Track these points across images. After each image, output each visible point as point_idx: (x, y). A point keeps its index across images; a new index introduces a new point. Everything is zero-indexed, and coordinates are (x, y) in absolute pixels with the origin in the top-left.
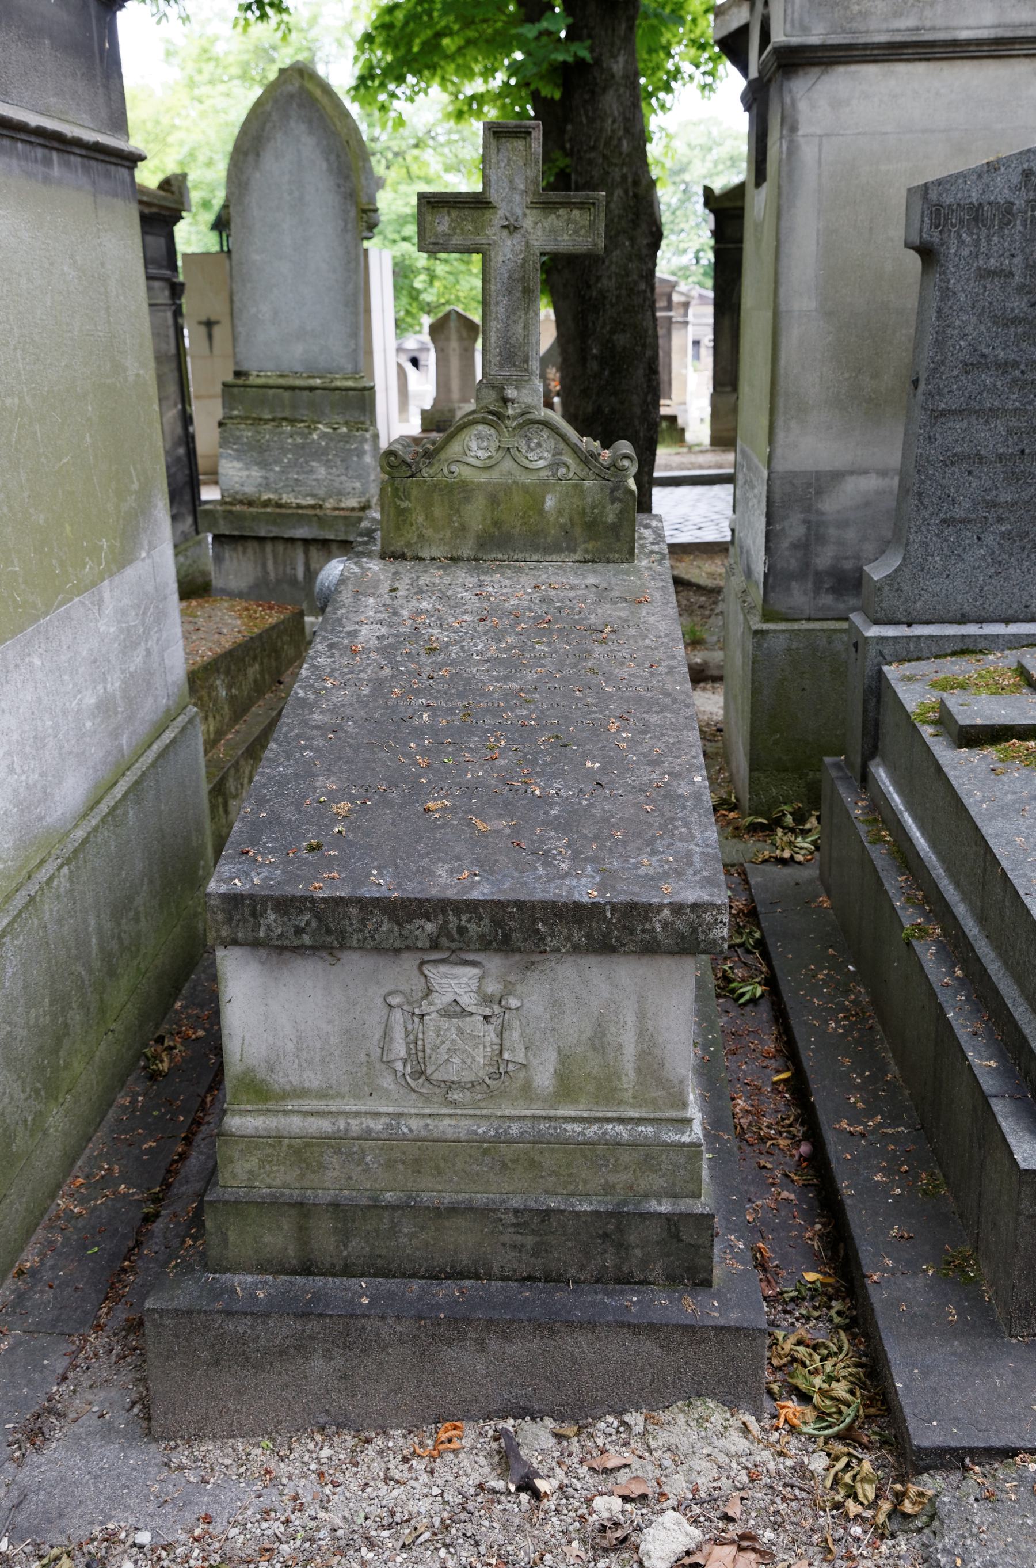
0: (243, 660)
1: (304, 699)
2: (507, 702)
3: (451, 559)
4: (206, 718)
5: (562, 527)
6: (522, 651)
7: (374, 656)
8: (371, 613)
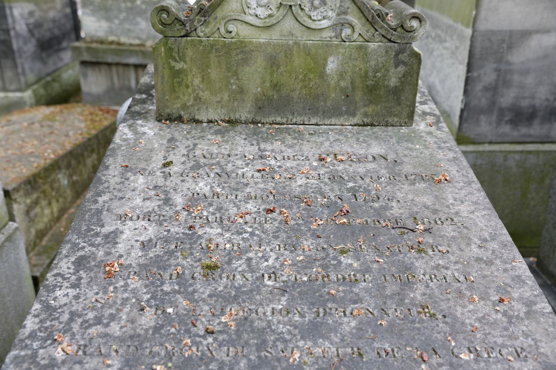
0: (82, 155)
3: (228, 122)
4: (50, 204)
5: (343, 90)
6: (325, 267)
7: (135, 283)
8: (138, 201)
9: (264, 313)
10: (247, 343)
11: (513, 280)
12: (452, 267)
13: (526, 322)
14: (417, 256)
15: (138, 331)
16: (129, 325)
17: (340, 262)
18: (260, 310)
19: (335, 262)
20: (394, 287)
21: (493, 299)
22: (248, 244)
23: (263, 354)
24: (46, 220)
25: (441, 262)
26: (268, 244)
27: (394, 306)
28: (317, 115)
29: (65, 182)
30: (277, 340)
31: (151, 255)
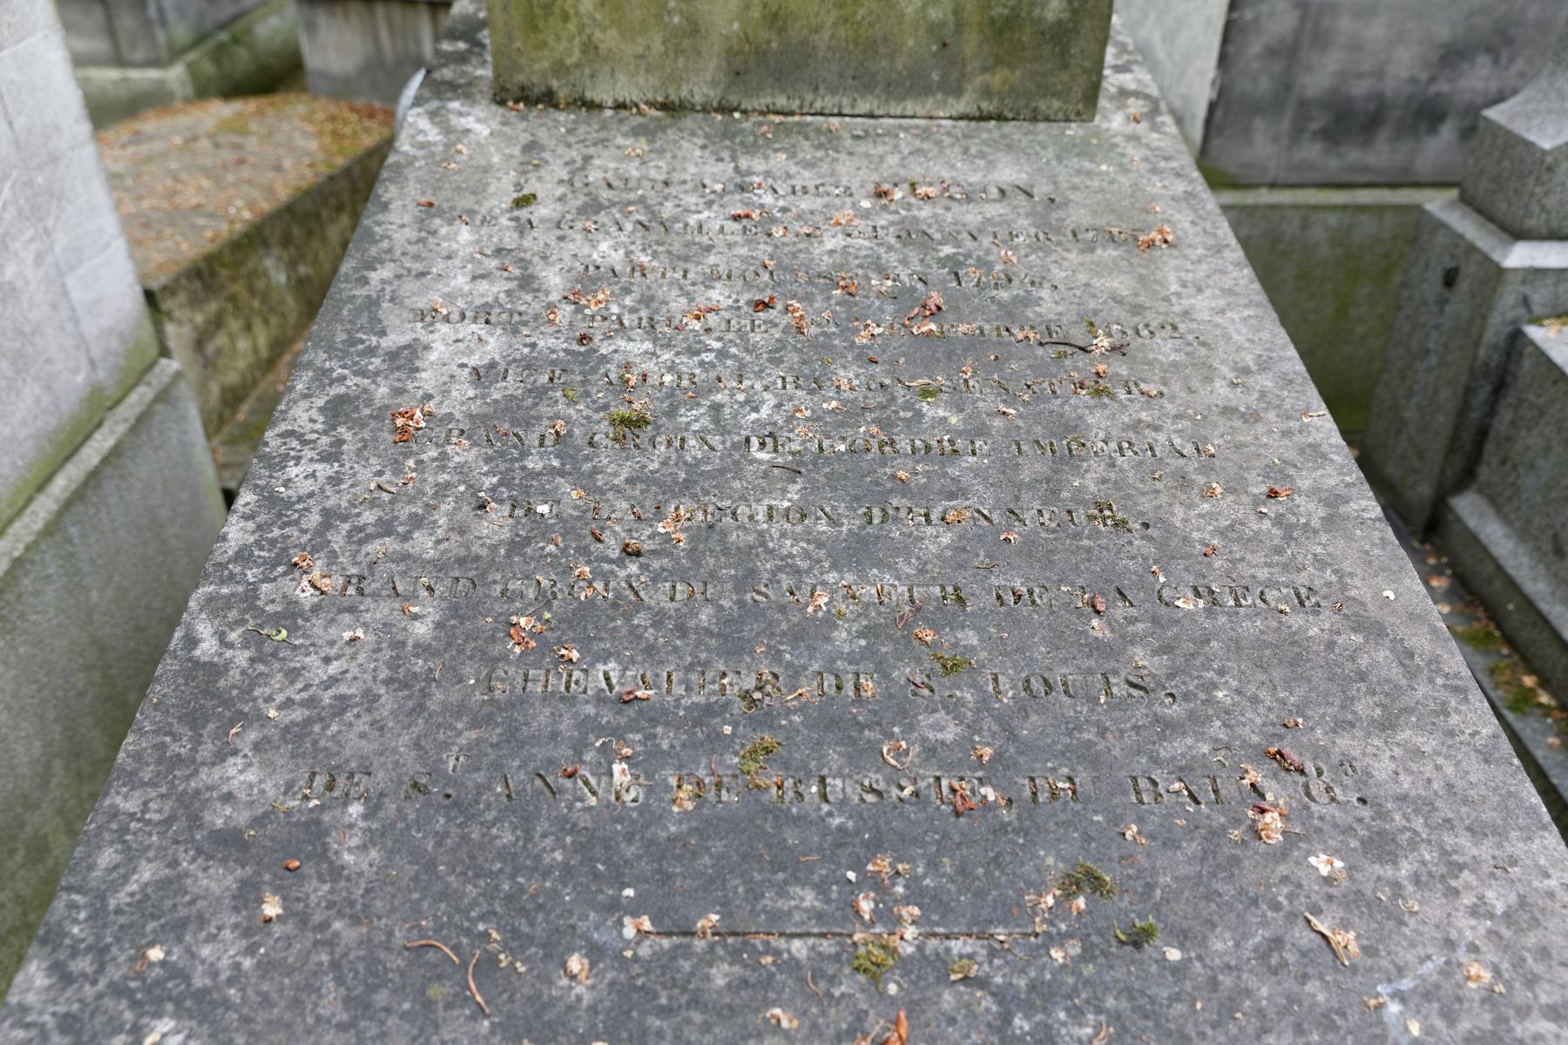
0: (317, 215)
1: (215, 670)
2: (882, 670)
3: (664, 107)
4: (248, 327)
5: (934, 29)
6: (885, 424)
7: (462, 453)
8: (461, 281)
9: (751, 517)
10: (713, 575)
11: (1302, 452)
12: (1168, 425)
13: (1324, 538)
14: (1092, 402)
15: (476, 549)
16: (454, 536)
17: (919, 415)
18: (742, 510)
19: (909, 414)
20: (1038, 466)
21: (1256, 491)
22: (713, 375)
23: (748, 597)
24: (242, 364)
25: (1144, 415)
26: (759, 375)
27: (1037, 505)
28: (872, 93)
29: (281, 278)
30: (780, 569)
31: (496, 396)
